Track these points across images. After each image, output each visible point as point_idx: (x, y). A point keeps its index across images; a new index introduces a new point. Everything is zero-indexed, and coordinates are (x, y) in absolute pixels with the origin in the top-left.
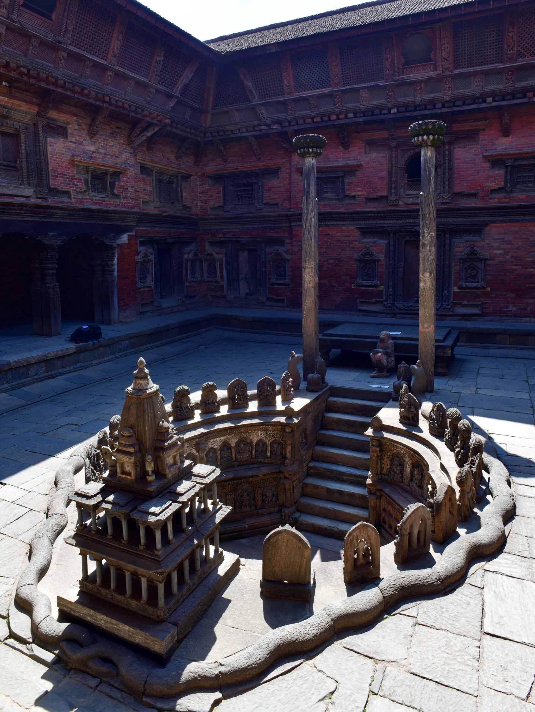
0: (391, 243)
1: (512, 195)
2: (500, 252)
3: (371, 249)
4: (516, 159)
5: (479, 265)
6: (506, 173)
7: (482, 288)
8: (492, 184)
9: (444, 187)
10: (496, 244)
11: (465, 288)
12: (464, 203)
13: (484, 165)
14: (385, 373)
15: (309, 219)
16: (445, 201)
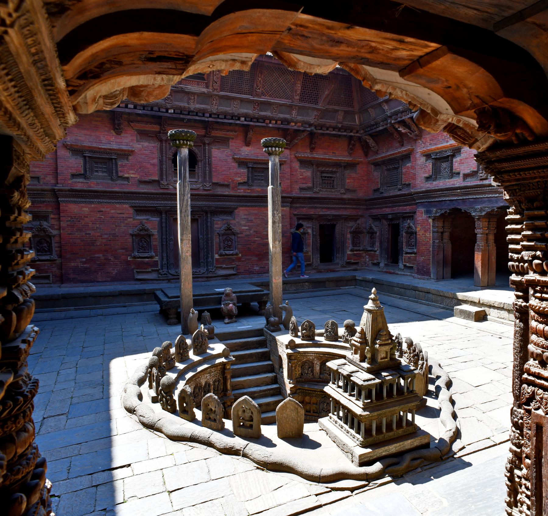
0: (164, 220)
1: (253, 188)
2: (246, 228)
3: (146, 225)
4: (255, 163)
5: (233, 237)
6: (248, 171)
7: (237, 254)
8: (239, 179)
9: (205, 177)
10: (243, 222)
11: (224, 255)
12: (220, 191)
13: (233, 164)
14: (234, 319)
15: (185, 199)
16: (207, 189)
